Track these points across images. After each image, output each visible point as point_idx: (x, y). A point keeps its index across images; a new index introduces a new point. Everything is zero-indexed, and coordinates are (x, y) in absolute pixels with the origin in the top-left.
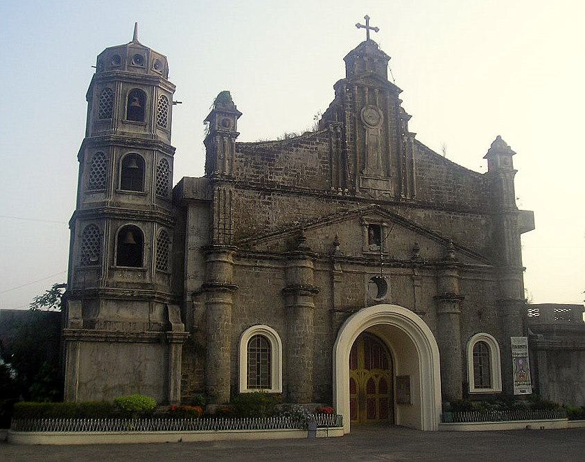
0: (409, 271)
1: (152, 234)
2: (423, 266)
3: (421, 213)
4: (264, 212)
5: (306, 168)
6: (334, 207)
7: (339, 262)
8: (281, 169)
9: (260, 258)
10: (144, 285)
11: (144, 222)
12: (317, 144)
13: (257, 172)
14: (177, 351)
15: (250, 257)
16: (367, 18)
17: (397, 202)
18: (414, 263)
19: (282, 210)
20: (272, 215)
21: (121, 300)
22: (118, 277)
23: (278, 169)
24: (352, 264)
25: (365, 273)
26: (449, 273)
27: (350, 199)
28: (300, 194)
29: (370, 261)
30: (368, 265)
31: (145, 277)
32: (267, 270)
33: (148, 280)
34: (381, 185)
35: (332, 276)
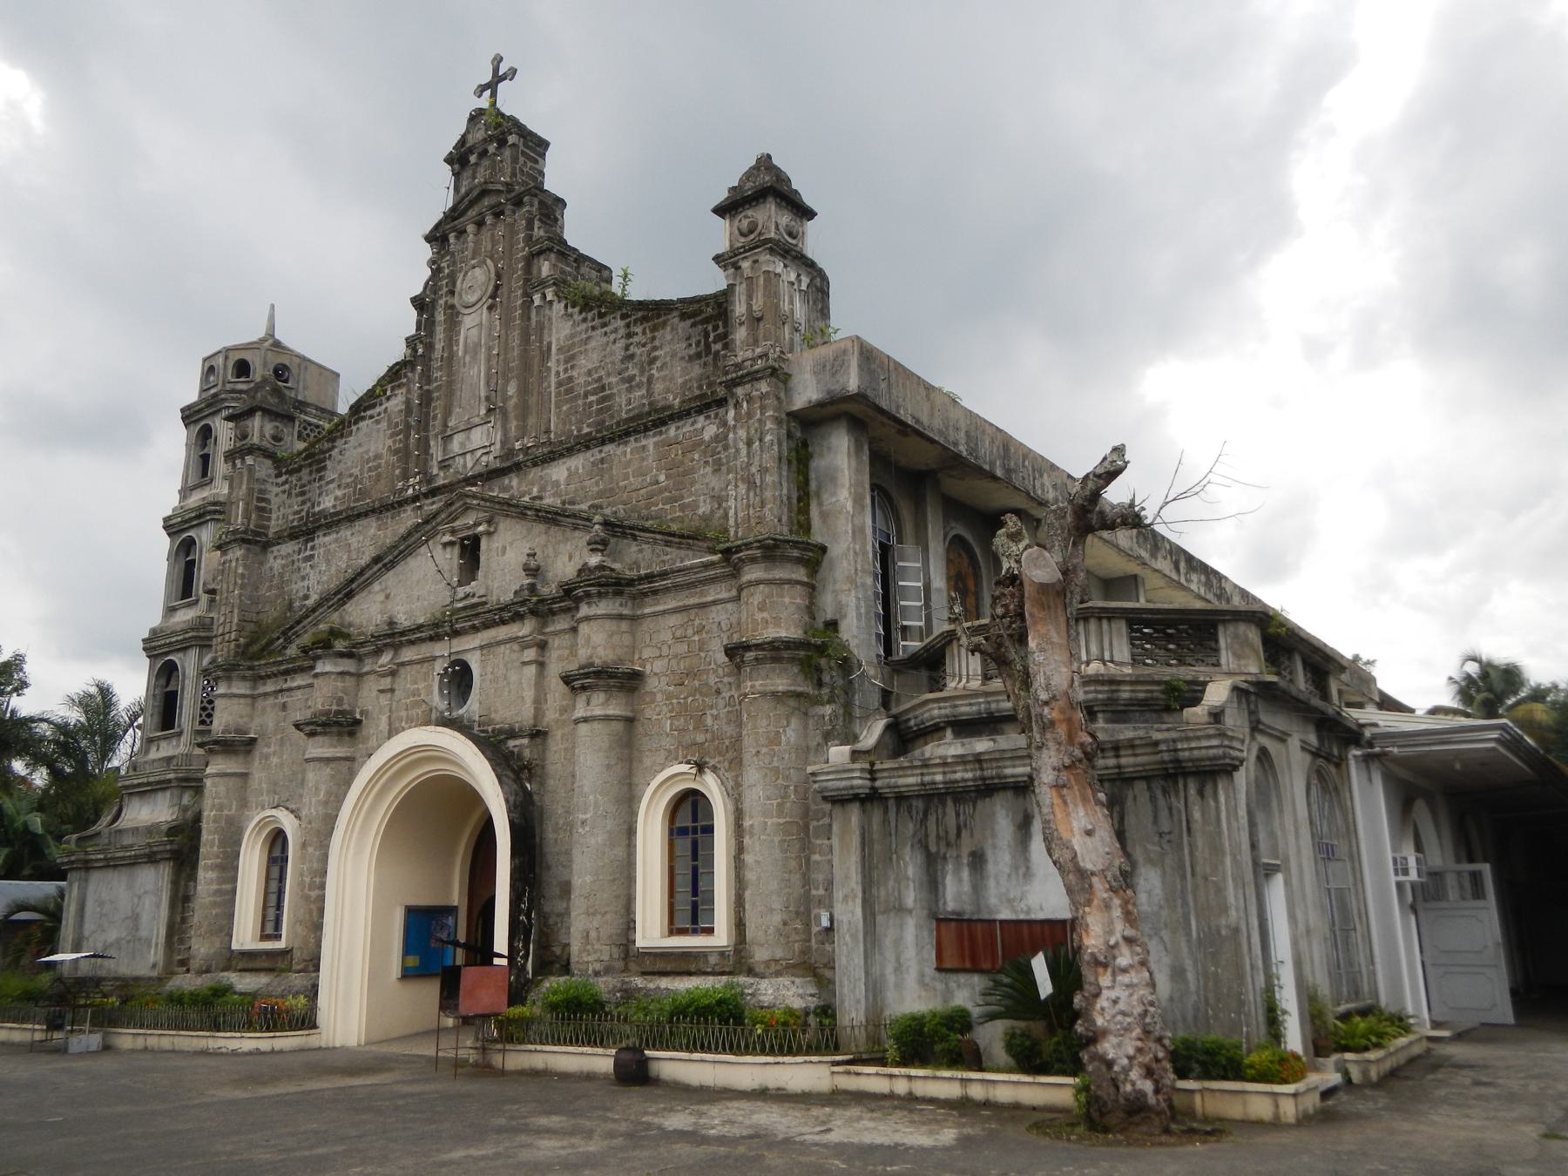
3: (559, 472)
4: (303, 578)
5: (368, 461)
6: (409, 518)
7: (385, 645)
8: (333, 480)
9: (287, 672)
11: (184, 649)
12: (388, 399)
13: (303, 503)
15: (275, 675)
16: (498, 60)
17: (511, 466)
19: (328, 561)
23: (328, 483)
24: (412, 643)
25: (434, 659)
27: (426, 496)
29: (439, 629)
31: (178, 746)
32: (299, 693)
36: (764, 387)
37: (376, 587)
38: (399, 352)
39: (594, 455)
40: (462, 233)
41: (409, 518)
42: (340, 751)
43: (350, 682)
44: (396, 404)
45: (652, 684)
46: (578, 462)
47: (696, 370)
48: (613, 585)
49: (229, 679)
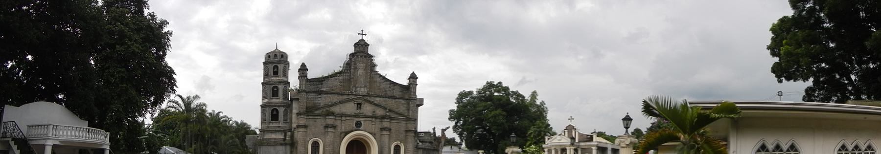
0: (370, 119)
1: (281, 110)
2: (376, 118)
3: (378, 99)
6: (345, 97)
10: (279, 127)
11: (279, 107)
14: (288, 147)
17: (368, 95)
18: (374, 117)
20: (321, 101)
21: (272, 132)
22: (271, 125)
26: (386, 120)
28: (331, 93)
29: (356, 116)
30: (355, 117)
31: (279, 124)
32: (320, 120)
33: (280, 125)
34: (362, 89)
35: (342, 121)
36: (415, 101)
37: (338, 106)
38: (338, 67)
39: (384, 99)
40: (357, 56)
41: (345, 97)
42: (334, 131)
43: (334, 120)
44: (341, 77)
45: (392, 131)
46: (381, 99)
47: (401, 93)
48: (391, 118)
49: (304, 115)
